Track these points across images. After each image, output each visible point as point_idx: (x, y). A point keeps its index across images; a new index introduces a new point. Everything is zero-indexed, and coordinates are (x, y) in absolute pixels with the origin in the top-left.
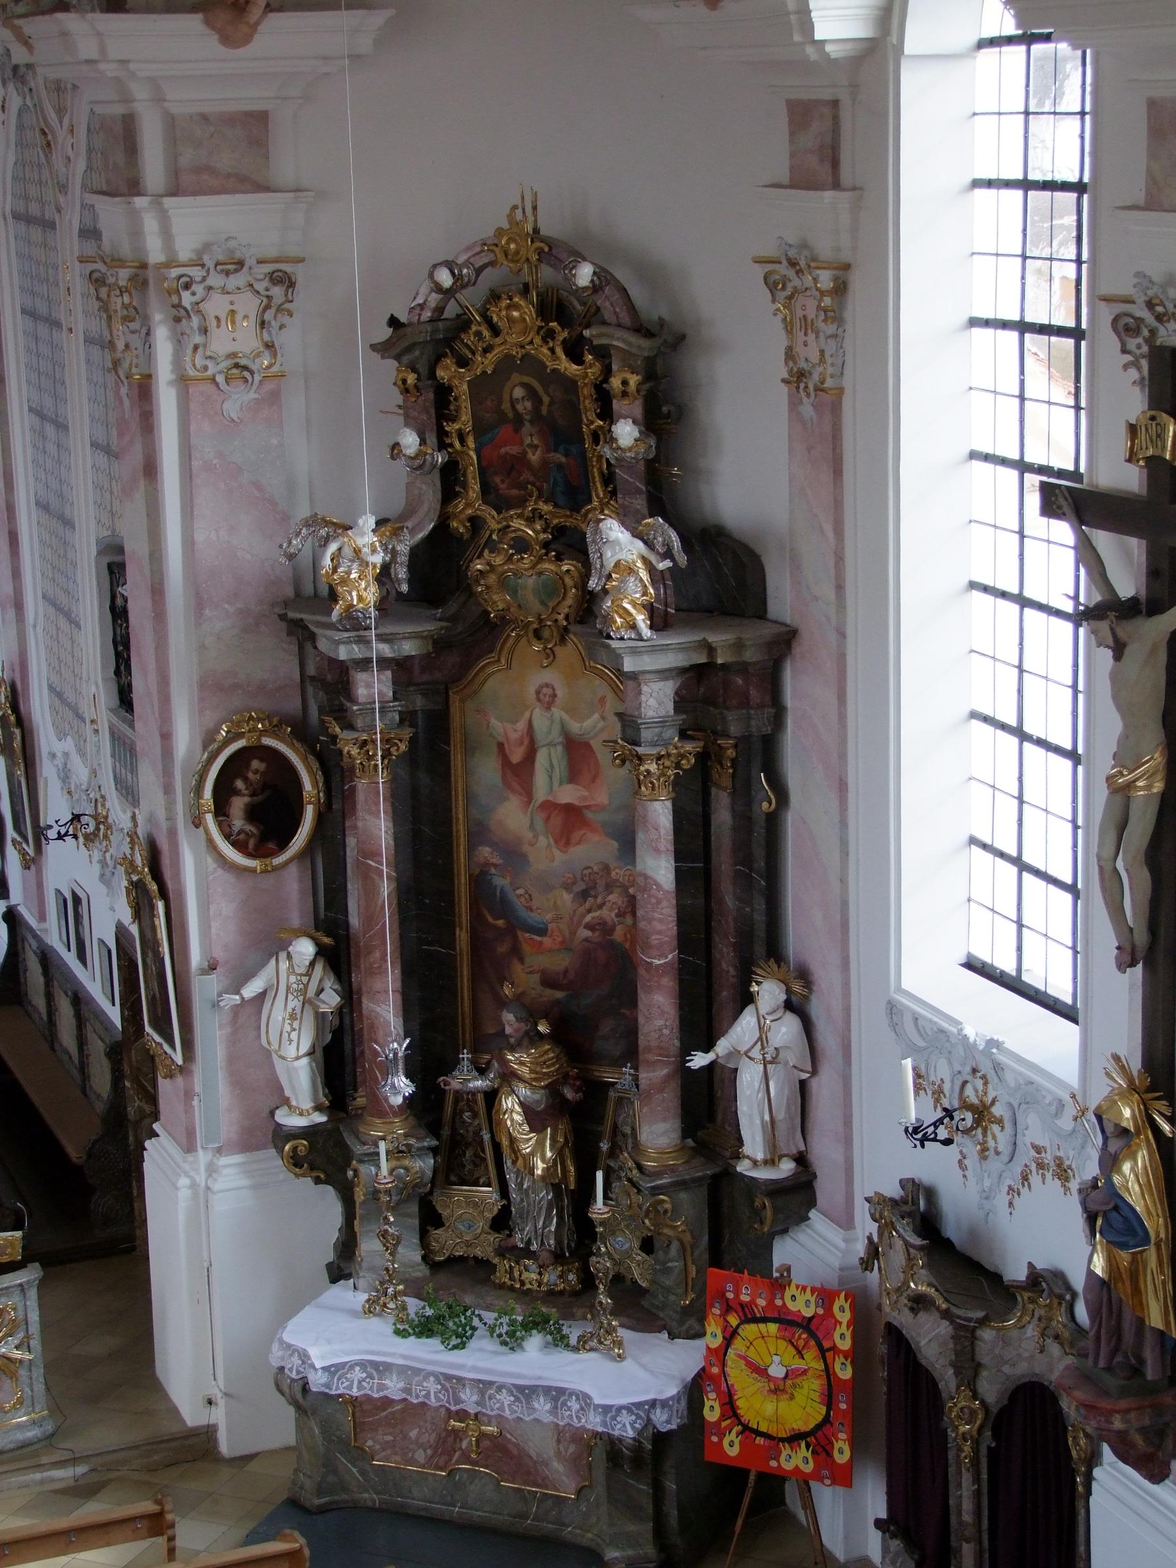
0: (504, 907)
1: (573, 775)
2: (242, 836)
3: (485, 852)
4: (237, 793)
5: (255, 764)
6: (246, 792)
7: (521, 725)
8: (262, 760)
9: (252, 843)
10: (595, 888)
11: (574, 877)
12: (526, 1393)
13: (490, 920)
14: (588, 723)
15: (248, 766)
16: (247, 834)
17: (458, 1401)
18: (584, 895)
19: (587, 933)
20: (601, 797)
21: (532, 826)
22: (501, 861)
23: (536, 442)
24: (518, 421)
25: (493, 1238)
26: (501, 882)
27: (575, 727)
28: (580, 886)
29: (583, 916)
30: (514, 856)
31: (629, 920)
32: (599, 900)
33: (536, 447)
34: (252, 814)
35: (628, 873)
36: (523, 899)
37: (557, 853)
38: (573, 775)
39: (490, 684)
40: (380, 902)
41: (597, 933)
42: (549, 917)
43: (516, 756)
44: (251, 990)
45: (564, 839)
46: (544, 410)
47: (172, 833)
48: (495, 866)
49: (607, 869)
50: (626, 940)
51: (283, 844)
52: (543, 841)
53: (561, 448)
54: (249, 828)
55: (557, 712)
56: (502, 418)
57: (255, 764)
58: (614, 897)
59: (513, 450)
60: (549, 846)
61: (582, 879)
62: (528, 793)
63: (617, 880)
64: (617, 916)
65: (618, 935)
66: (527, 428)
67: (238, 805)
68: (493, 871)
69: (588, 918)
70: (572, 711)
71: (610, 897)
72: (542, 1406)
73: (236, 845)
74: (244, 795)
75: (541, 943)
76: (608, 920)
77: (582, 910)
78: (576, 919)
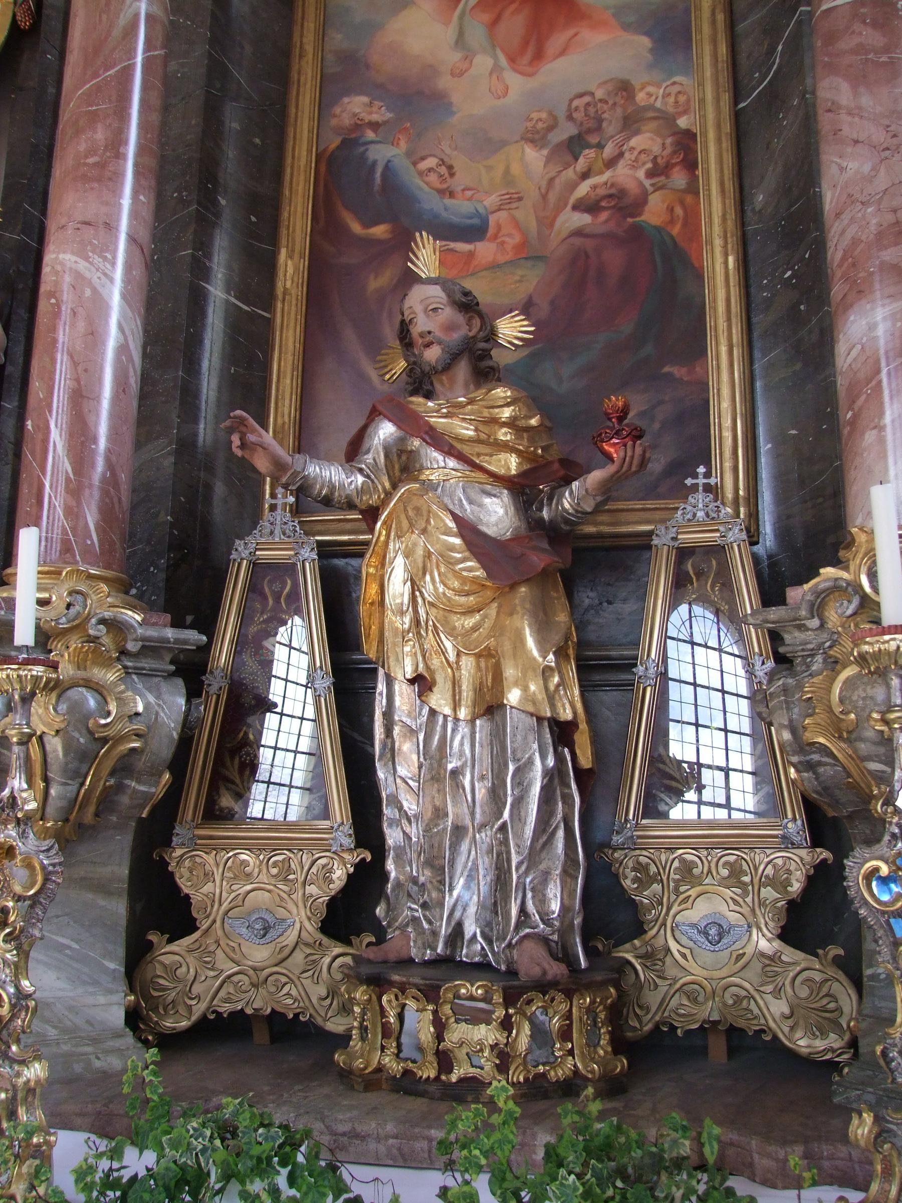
3: (356, 106)
10: (599, 129)
11: (550, 114)
13: (356, 227)
18: (574, 146)
19: (583, 219)
21: (460, 41)
22: (389, 115)
25: (336, 956)
26: (382, 153)
28: (566, 131)
29: (573, 186)
30: (417, 100)
31: (679, 179)
32: (609, 150)
35: (676, 88)
36: (433, 178)
37: (515, 81)
40: (123, 20)
41: (604, 216)
42: (491, 201)
48: (375, 126)
49: (625, 88)
50: (672, 222)
52: (483, 63)
58: (647, 141)
60: (496, 69)
61: (570, 118)
63: (651, 107)
64: (650, 174)
65: (654, 212)
68: (370, 135)
69: (583, 189)
71: (633, 142)
75: (471, 255)
76: (631, 187)
77: (570, 174)
78: (552, 197)
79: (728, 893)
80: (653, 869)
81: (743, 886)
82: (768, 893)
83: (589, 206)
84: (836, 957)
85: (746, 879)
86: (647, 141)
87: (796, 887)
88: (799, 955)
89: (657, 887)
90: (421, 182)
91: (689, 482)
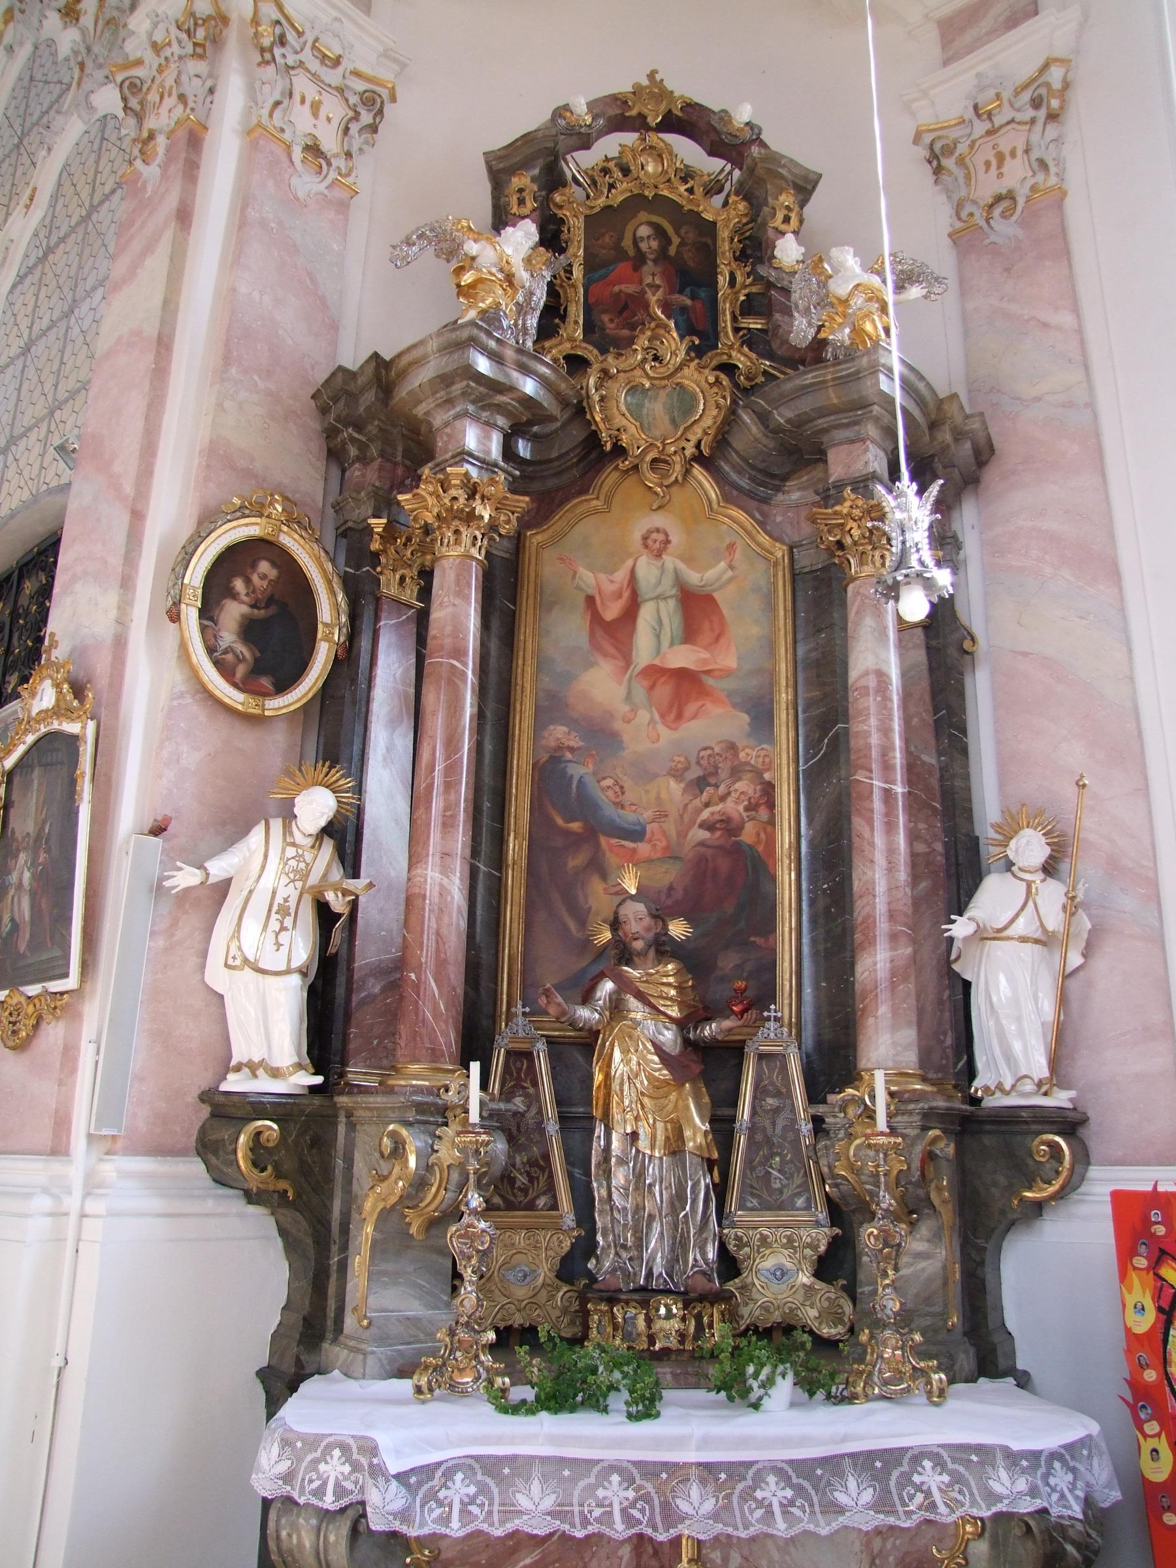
0: (584, 807)
1: (689, 634)
3: (558, 732)
4: (234, 596)
5: (264, 566)
6: (245, 599)
7: (621, 575)
8: (274, 564)
9: (241, 671)
10: (715, 774)
11: (686, 758)
12: (814, 1475)
13: (560, 821)
14: (710, 574)
15: (254, 566)
16: (237, 656)
17: (670, 1515)
18: (701, 784)
19: (704, 835)
20: (729, 661)
21: (629, 697)
22: (581, 744)
23: (658, 282)
24: (640, 259)
26: (576, 771)
27: (693, 578)
28: (695, 773)
29: (699, 812)
30: (601, 735)
31: (763, 814)
32: (722, 789)
33: (658, 287)
34: (249, 630)
35: (763, 753)
36: (610, 793)
38: (689, 634)
39: (584, 528)
41: (718, 834)
42: (647, 815)
43: (611, 612)
44: (218, 868)
45: (675, 712)
46: (672, 251)
47: (120, 644)
48: (571, 749)
50: (759, 842)
51: (283, 686)
52: (644, 716)
53: (688, 290)
54: (241, 648)
55: (669, 561)
56: (621, 255)
57: (264, 566)
59: (630, 289)
60: (652, 721)
61: (698, 763)
62: (627, 659)
63: (748, 763)
64: (747, 809)
65: (748, 835)
66: (649, 267)
68: (569, 756)
69: (705, 814)
70: (689, 560)
71: (738, 785)
72: (854, 1495)
73: (218, 664)
74: (243, 603)
75: (634, 851)
76: (735, 815)
77: (697, 802)
78: (686, 818)
79: (786, 1252)
80: (745, 1239)
81: (794, 1248)
82: (808, 1252)
83: (708, 826)
84: (843, 1286)
85: (796, 1244)
86: (745, 786)
87: (822, 1248)
88: (824, 1285)
89: (747, 1249)
90: (602, 794)
91: (766, 1014)
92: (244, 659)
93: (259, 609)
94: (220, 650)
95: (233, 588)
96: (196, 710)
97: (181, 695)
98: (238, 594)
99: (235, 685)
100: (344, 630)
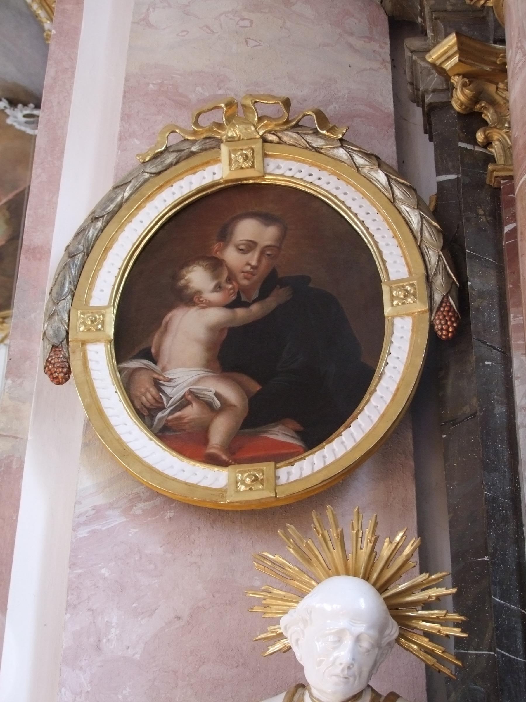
2: (192, 411)
4: (189, 299)
5: (247, 229)
6: (215, 297)
8: (266, 218)
9: (220, 430)
15: (225, 235)
16: (209, 405)
34: (228, 353)
51: (316, 433)
67: (187, 336)
74: (209, 305)
92: (226, 405)
93: (246, 305)
94: (169, 405)
95: (186, 287)
96: (145, 538)
97: (98, 513)
98: (199, 293)
99: (213, 460)
100: (439, 281)
